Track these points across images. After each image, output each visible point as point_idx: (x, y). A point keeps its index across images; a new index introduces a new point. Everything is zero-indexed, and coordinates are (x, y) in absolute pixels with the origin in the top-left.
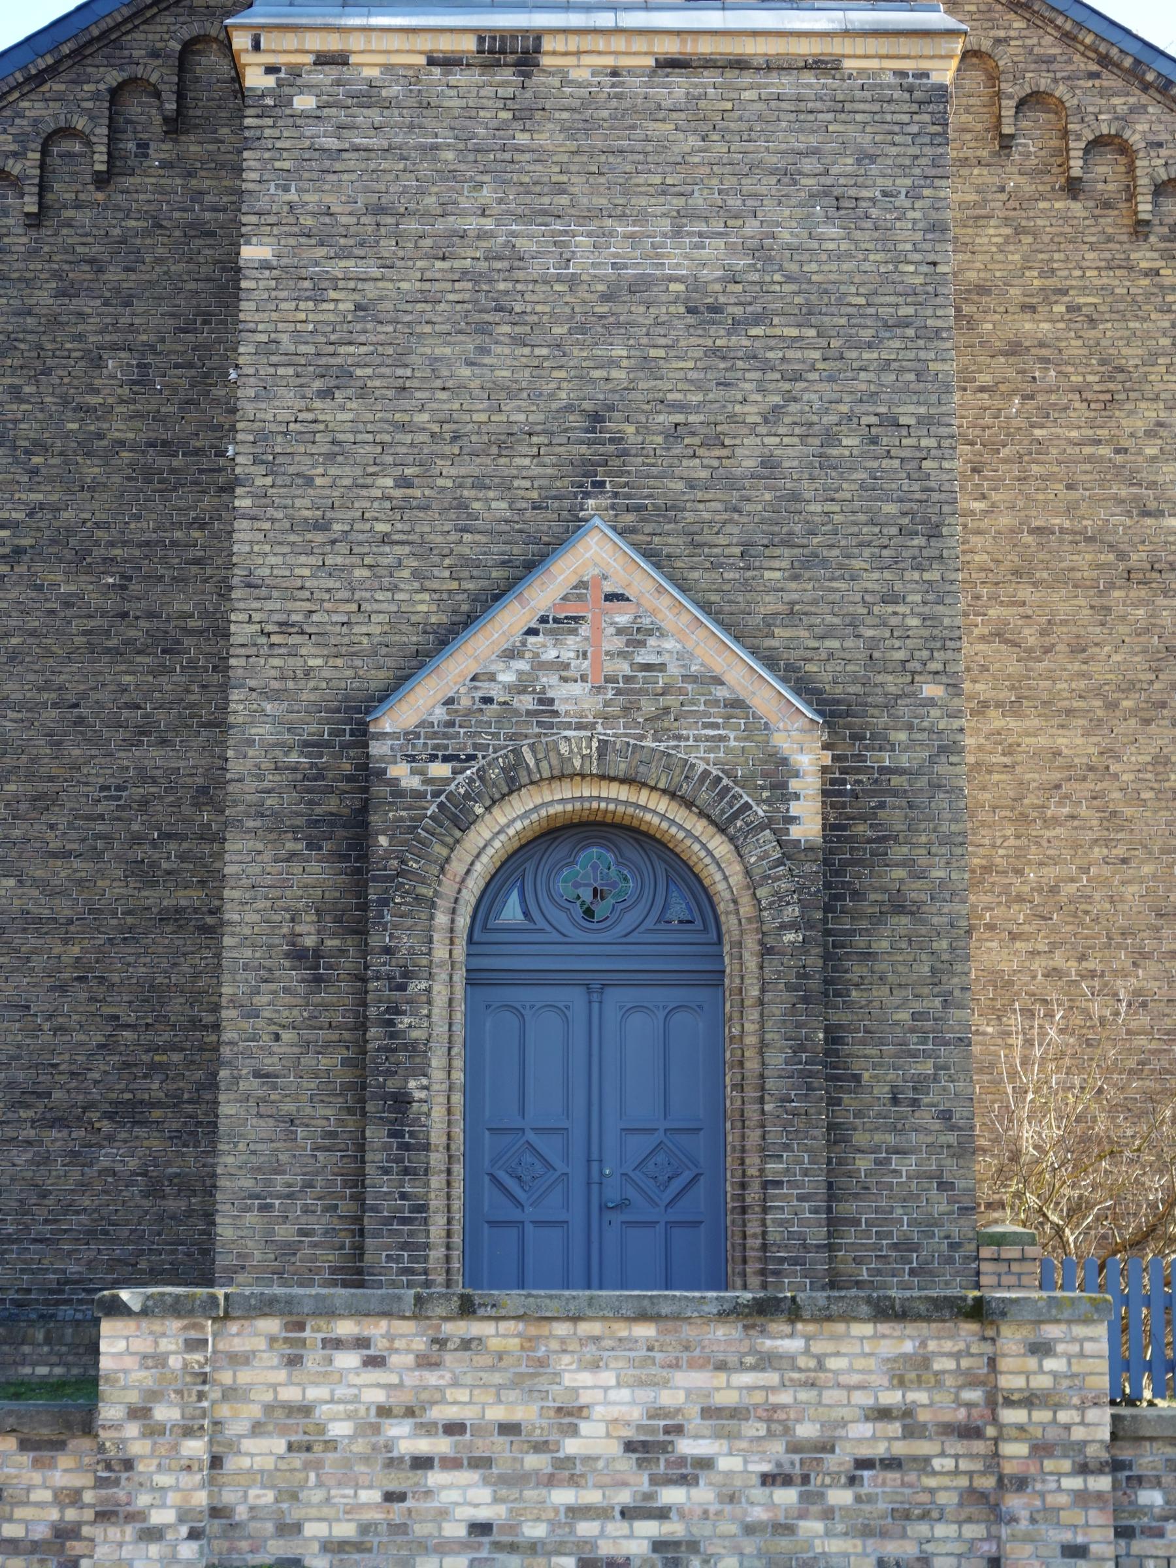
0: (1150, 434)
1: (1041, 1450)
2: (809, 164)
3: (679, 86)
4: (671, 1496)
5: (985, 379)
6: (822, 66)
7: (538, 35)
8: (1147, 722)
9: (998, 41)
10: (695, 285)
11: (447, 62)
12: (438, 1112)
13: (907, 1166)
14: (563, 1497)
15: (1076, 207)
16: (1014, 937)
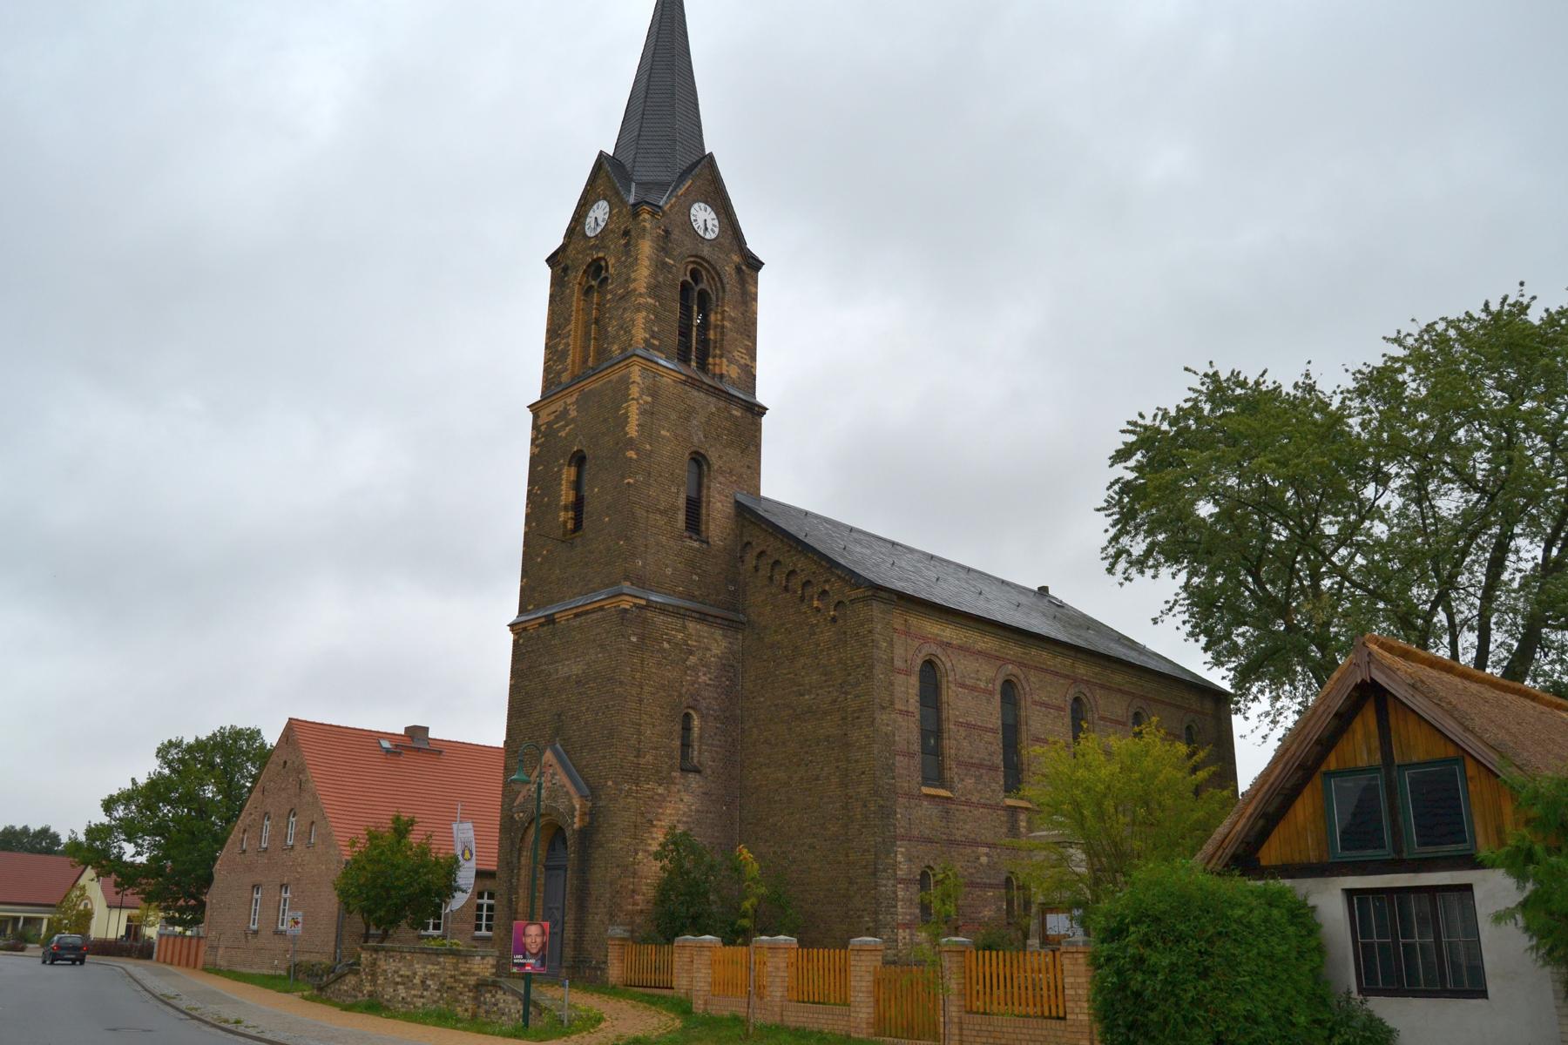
1: (464, 987)
3: (576, 623)
4: (425, 993)
5: (765, 657)
6: (601, 608)
8: (799, 766)
10: (577, 675)
11: (541, 625)
12: (521, 904)
13: (597, 918)
14: (413, 992)
15: (788, 596)
16: (766, 841)
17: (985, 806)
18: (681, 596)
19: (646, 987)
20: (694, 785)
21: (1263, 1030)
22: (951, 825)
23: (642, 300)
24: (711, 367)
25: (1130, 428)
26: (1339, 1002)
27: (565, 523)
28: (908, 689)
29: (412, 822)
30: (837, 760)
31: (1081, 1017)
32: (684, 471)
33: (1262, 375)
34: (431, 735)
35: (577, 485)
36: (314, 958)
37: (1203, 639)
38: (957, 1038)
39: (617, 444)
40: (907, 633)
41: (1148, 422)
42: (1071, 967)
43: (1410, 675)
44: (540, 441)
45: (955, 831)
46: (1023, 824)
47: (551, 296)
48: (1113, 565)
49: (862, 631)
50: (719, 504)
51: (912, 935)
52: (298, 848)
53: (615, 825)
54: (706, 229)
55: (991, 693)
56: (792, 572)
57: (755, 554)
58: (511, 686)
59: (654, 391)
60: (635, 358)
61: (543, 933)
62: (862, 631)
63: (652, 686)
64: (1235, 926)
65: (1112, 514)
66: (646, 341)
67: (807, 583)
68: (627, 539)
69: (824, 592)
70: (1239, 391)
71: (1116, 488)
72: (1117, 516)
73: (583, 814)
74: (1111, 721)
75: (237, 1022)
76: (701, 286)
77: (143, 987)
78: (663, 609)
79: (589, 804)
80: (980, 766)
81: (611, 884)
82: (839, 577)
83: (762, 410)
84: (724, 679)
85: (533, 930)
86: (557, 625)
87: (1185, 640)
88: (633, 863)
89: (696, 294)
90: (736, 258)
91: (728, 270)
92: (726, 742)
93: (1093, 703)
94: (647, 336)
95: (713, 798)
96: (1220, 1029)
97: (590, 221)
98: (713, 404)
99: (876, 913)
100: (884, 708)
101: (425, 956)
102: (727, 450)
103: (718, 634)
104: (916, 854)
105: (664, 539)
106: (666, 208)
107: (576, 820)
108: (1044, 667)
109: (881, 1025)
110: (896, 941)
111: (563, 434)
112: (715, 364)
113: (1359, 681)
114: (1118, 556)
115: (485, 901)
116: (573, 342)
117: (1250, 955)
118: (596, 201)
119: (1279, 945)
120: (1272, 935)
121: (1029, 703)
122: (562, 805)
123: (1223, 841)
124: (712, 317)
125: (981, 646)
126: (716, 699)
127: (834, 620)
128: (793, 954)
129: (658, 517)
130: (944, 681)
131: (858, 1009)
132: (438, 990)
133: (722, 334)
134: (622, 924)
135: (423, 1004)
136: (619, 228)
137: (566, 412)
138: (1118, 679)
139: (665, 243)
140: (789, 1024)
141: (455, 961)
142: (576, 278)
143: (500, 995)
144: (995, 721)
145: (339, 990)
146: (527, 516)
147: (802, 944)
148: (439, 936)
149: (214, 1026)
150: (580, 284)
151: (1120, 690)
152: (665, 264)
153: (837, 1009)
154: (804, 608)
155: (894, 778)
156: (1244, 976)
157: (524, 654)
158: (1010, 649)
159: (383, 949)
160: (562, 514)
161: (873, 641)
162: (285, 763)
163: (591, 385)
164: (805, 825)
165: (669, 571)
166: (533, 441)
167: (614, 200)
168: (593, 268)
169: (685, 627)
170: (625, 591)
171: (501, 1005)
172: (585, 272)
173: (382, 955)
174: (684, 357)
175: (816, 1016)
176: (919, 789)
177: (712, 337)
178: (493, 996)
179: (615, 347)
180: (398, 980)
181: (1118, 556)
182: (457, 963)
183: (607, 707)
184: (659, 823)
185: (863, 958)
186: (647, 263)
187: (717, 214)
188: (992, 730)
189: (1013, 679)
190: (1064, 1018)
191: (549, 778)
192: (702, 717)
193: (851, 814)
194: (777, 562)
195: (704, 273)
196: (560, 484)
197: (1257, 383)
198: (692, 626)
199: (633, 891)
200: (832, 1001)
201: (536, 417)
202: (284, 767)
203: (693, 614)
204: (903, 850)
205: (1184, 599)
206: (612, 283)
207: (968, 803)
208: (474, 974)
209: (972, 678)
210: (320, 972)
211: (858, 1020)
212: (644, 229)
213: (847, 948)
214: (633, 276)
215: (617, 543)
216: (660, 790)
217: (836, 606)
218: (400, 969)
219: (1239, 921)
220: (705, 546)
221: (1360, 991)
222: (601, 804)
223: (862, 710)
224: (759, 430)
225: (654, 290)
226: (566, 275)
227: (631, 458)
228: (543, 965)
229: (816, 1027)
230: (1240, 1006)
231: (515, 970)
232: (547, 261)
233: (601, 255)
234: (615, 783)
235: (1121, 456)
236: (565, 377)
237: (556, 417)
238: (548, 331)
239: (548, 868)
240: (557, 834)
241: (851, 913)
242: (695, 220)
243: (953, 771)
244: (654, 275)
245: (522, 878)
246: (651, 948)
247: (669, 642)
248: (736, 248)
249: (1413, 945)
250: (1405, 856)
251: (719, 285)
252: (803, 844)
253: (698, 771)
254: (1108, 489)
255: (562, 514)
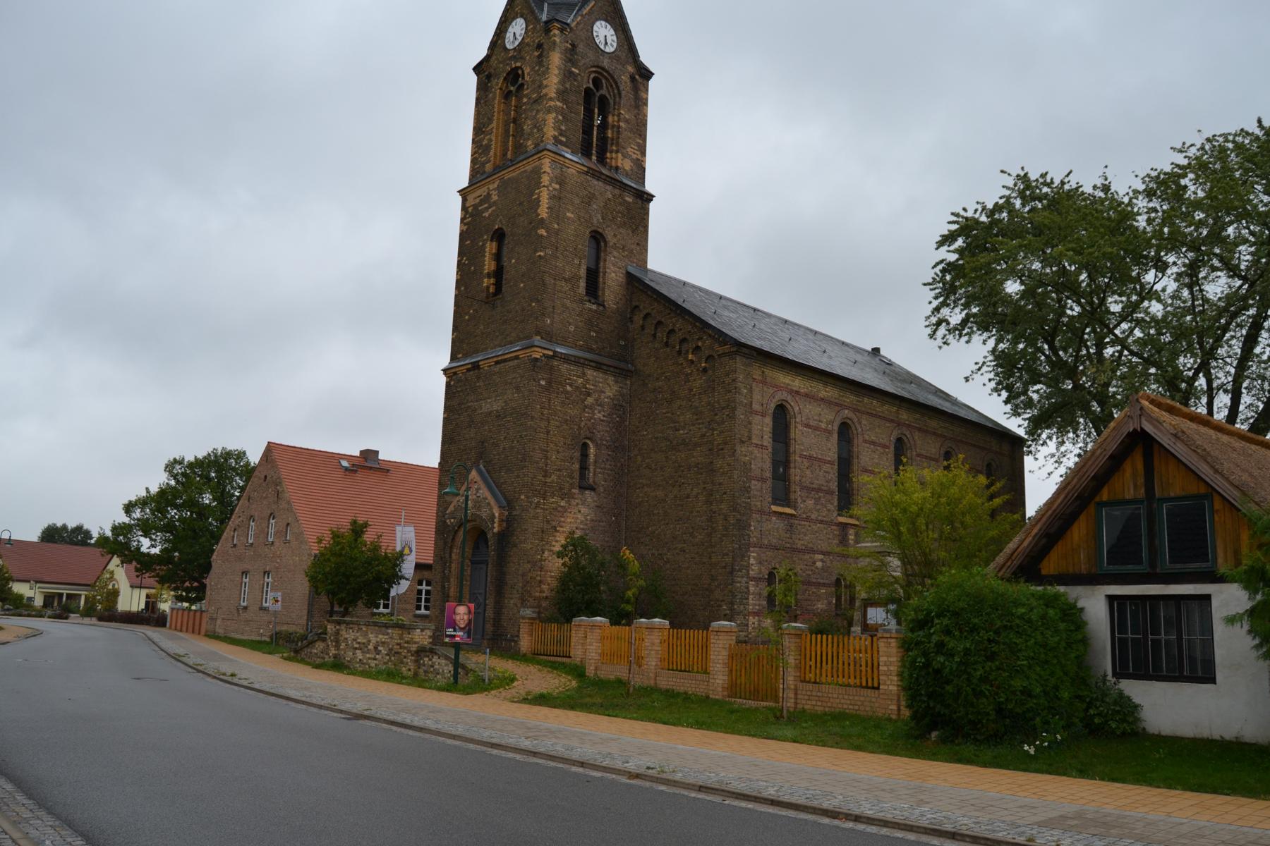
0: (679, 408)
2: (514, 381)
3: (496, 369)
4: (377, 656)
5: (648, 399)
6: (517, 358)
7: (478, 361)
8: (673, 487)
9: (653, 309)
10: (497, 411)
11: (468, 370)
12: (452, 590)
14: (368, 656)
15: (668, 349)
16: (646, 545)
17: (821, 522)
18: (580, 348)
19: (550, 655)
20: (589, 500)
21: (1035, 701)
22: (794, 536)
23: (552, 103)
24: (608, 160)
25: (955, 219)
26: (1097, 683)
27: (488, 287)
28: (763, 427)
29: (366, 525)
30: (704, 483)
31: (891, 688)
32: (584, 245)
33: (1067, 176)
34: (381, 457)
35: (498, 257)
36: (292, 629)
37: (1004, 394)
38: (793, 701)
39: (531, 223)
40: (764, 382)
41: (970, 214)
42: (886, 649)
43: (1174, 426)
44: (468, 220)
45: (797, 541)
46: (852, 537)
47: (477, 99)
48: (935, 332)
49: (727, 380)
50: (613, 274)
51: (759, 621)
52: (277, 544)
53: (526, 530)
54: (606, 43)
55: (830, 433)
56: (672, 331)
57: (642, 316)
58: (444, 418)
59: (561, 180)
60: (545, 152)
61: (470, 612)
62: (727, 380)
63: (556, 420)
64: (1017, 621)
65: (935, 289)
66: (555, 138)
67: (683, 341)
68: (538, 301)
69: (698, 348)
70: (1045, 190)
71: (940, 267)
72: (940, 290)
73: (501, 521)
74: (926, 457)
75: (233, 675)
76: (604, 92)
77: (159, 647)
78: (566, 359)
79: (506, 513)
80: (818, 490)
81: (523, 575)
82: (710, 336)
83: (649, 198)
84: (615, 416)
85: (462, 610)
86: (482, 371)
87: (990, 395)
88: (541, 560)
89: (597, 99)
90: (630, 69)
91: (624, 79)
92: (615, 466)
93: (912, 443)
94: (556, 134)
95: (605, 510)
96: (1002, 700)
97: (509, 35)
98: (610, 192)
99: (732, 603)
100: (743, 442)
101: (377, 628)
102: (621, 230)
103: (611, 379)
104: (765, 558)
105: (567, 302)
106: (573, 25)
107: (496, 525)
108: (874, 412)
109: (733, 689)
110: (747, 625)
111: (486, 214)
112: (612, 158)
113: (1131, 430)
114: (939, 323)
115: (424, 587)
116: (494, 139)
117: (1029, 643)
118: (514, 19)
119: (1052, 637)
120: (1047, 629)
121: (861, 440)
122: (484, 513)
123: (1012, 554)
124: (610, 119)
125: (823, 394)
126: (607, 431)
127: (705, 370)
128: (666, 633)
129: (563, 284)
130: (793, 421)
131: (715, 677)
132: (387, 655)
133: (618, 132)
134: (533, 607)
135: (376, 665)
136: (534, 42)
137: (489, 195)
138: (933, 424)
139: (571, 55)
140: (661, 686)
141: (400, 632)
142: (498, 84)
143: (435, 659)
144: (833, 455)
145: (311, 653)
146: (458, 282)
147: (672, 625)
148: (387, 614)
149: (215, 677)
150: (501, 89)
151: (934, 434)
152: (572, 72)
153: (699, 676)
154: (681, 360)
155: (749, 498)
156: (1023, 660)
157: (455, 393)
158: (846, 397)
159: (344, 622)
160: (485, 280)
161: (736, 388)
162: (266, 477)
163: (509, 174)
164: (677, 533)
165: (572, 328)
166: (462, 220)
167: (530, 18)
168: (511, 76)
169: (584, 374)
170: (536, 343)
171: (436, 667)
172: (505, 79)
173: (343, 627)
174: (586, 152)
175: (682, 681)
176: (770, 508)
177: (610, 135)
178: (430, 660)
179: (530, 143)
180: (357, 646)
181: (939, 323)
182: (402, 634)
183: (521, 436)
184: (562, 529)
185: (720, 637)
186: (556, 72)
187: (615, 31)
188: (829, 462)
189: (848, 421)
190: (878, 688)
191: (474, 492)
192: (597, 445)
193: (714, 525)
194: (660, 323)
195: (604, 81)
196: (485, 256)
197: (1063, 183)
198: (590, 373)
199: (540, 582)
200: (695, 670)
201: (464, 200)
202: (265, 481)
203: (591, 364)
204: (755, 555)
205: (991, 361)
206: (527, 89)
207: (808, 519)
208: (415, 643)
209: (816, 420)
210: (296, 639)
211: (716, 685)
212: (554, 42)
213: (708, 629)
214: (545, 82)
215: (530, 305)
216: (563, 503)
217: (706, 360)
218: (357, 638)
219: (1021, 617)
220: (601, 308)
221: (1115, 674)
222: (515, 513)
223: (725, 443)
224: (647, 214)
225: (562, 94)
226: (489, 81)
227: (542, 235)
228: (469, 637)
229: (682, 689)
230: (1018, 683)
231: (447, 640)
232: (475, 69)
233: (518, 64)
234: (527, 497)
235: (947, 240)
236: (489, 167)
237: (481, 200)
238: (475, 128)
239: (473, 562)
240: (480, 536)
241: (712, 603)
242: (597, 36)
243: (797, 493)
244: (562, 82)
245: (453, 569)
246: (554, 626)
247: (571, 386)
248: (631, 60)
249: (1160, 641)
250: (1158, 570)
251: (616, 91)
252: (675, 549)
253: (592, 489)
254: (933, 268)
255: (485, 280)
